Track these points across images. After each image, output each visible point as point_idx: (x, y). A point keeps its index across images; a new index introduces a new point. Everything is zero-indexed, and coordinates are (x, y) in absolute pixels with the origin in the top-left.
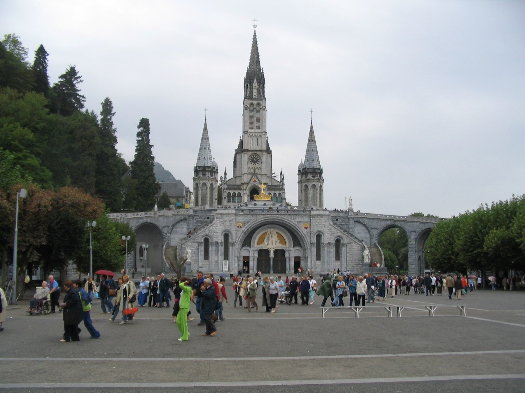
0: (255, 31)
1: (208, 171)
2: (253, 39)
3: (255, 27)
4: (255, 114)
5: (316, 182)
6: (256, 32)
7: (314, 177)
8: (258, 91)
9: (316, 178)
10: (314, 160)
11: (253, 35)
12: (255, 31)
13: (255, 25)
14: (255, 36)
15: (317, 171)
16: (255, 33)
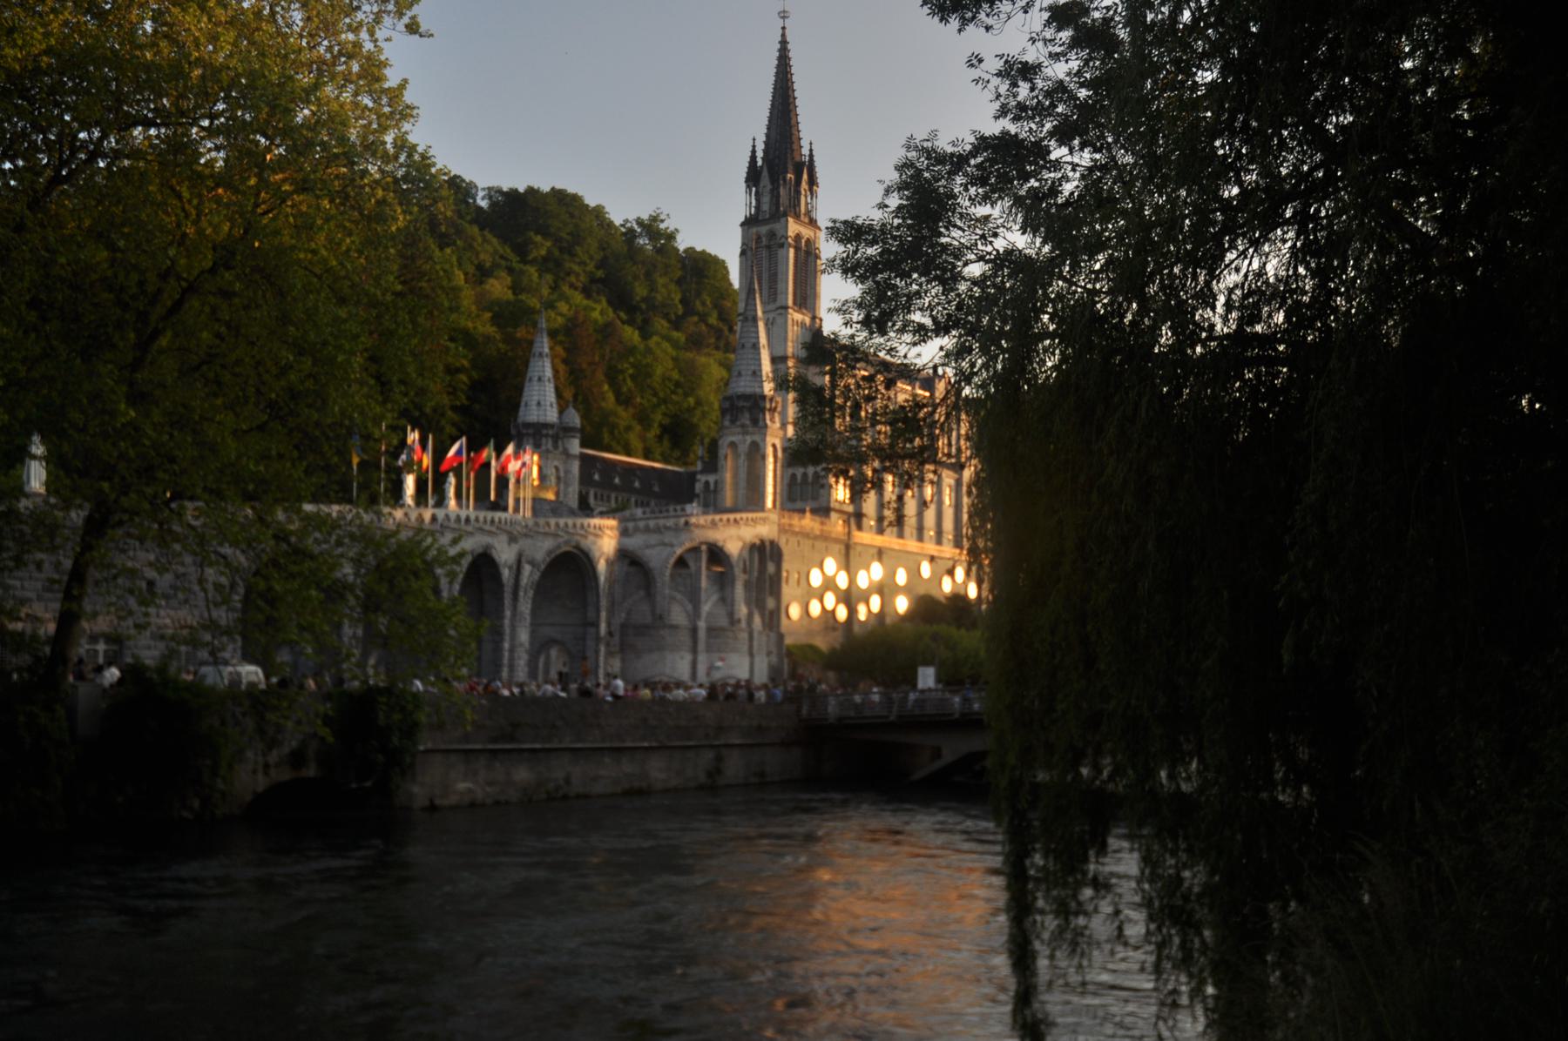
0: (784, 28)
1: (528, 434)
2: (780, 50)
3: (784, 18)
4: (765, 263)
5: (739, 433)
6: (787, 31)
7: (733, 422)
8: (771, 199)
9: (738, 423)
10: (743, 373)
11: (780, 39)
12: (784, 28)
13: (784, 12)
14: (784, 43)
15: (741, 404)
16: (783, 35)
